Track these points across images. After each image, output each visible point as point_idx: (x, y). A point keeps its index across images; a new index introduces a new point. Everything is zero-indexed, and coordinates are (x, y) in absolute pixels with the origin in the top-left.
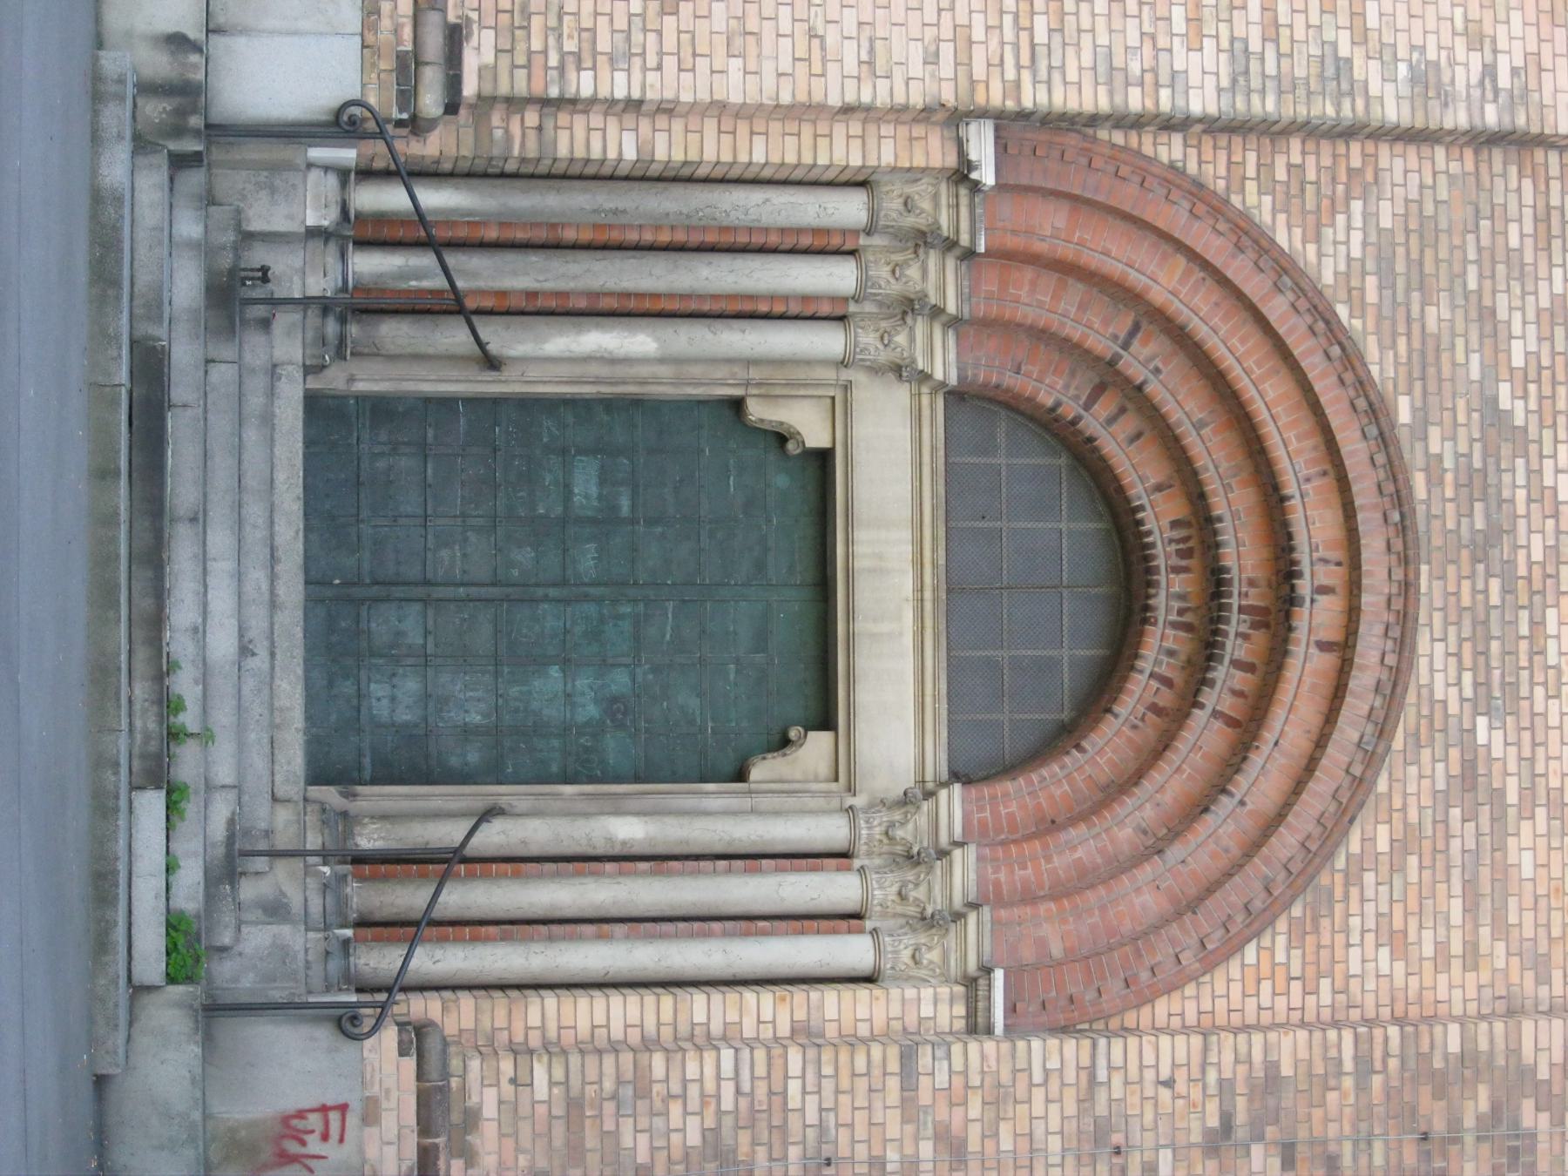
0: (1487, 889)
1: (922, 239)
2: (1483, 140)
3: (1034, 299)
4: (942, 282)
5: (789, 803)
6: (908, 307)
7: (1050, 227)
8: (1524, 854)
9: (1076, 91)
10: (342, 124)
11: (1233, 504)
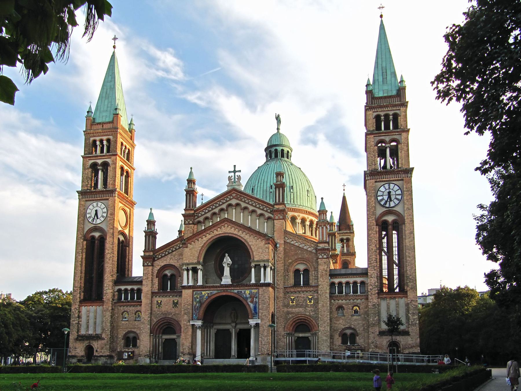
0: (178, 314)
1: (155, 336)
2: (151, 314)
3: (158, 332)
4: (157, 335)
5: (177, 340)
6: (158, 337)
7: (155, 332)
8: (177, 313)
9: (149, 331)
10: (150, 359)
11: (165, 324)
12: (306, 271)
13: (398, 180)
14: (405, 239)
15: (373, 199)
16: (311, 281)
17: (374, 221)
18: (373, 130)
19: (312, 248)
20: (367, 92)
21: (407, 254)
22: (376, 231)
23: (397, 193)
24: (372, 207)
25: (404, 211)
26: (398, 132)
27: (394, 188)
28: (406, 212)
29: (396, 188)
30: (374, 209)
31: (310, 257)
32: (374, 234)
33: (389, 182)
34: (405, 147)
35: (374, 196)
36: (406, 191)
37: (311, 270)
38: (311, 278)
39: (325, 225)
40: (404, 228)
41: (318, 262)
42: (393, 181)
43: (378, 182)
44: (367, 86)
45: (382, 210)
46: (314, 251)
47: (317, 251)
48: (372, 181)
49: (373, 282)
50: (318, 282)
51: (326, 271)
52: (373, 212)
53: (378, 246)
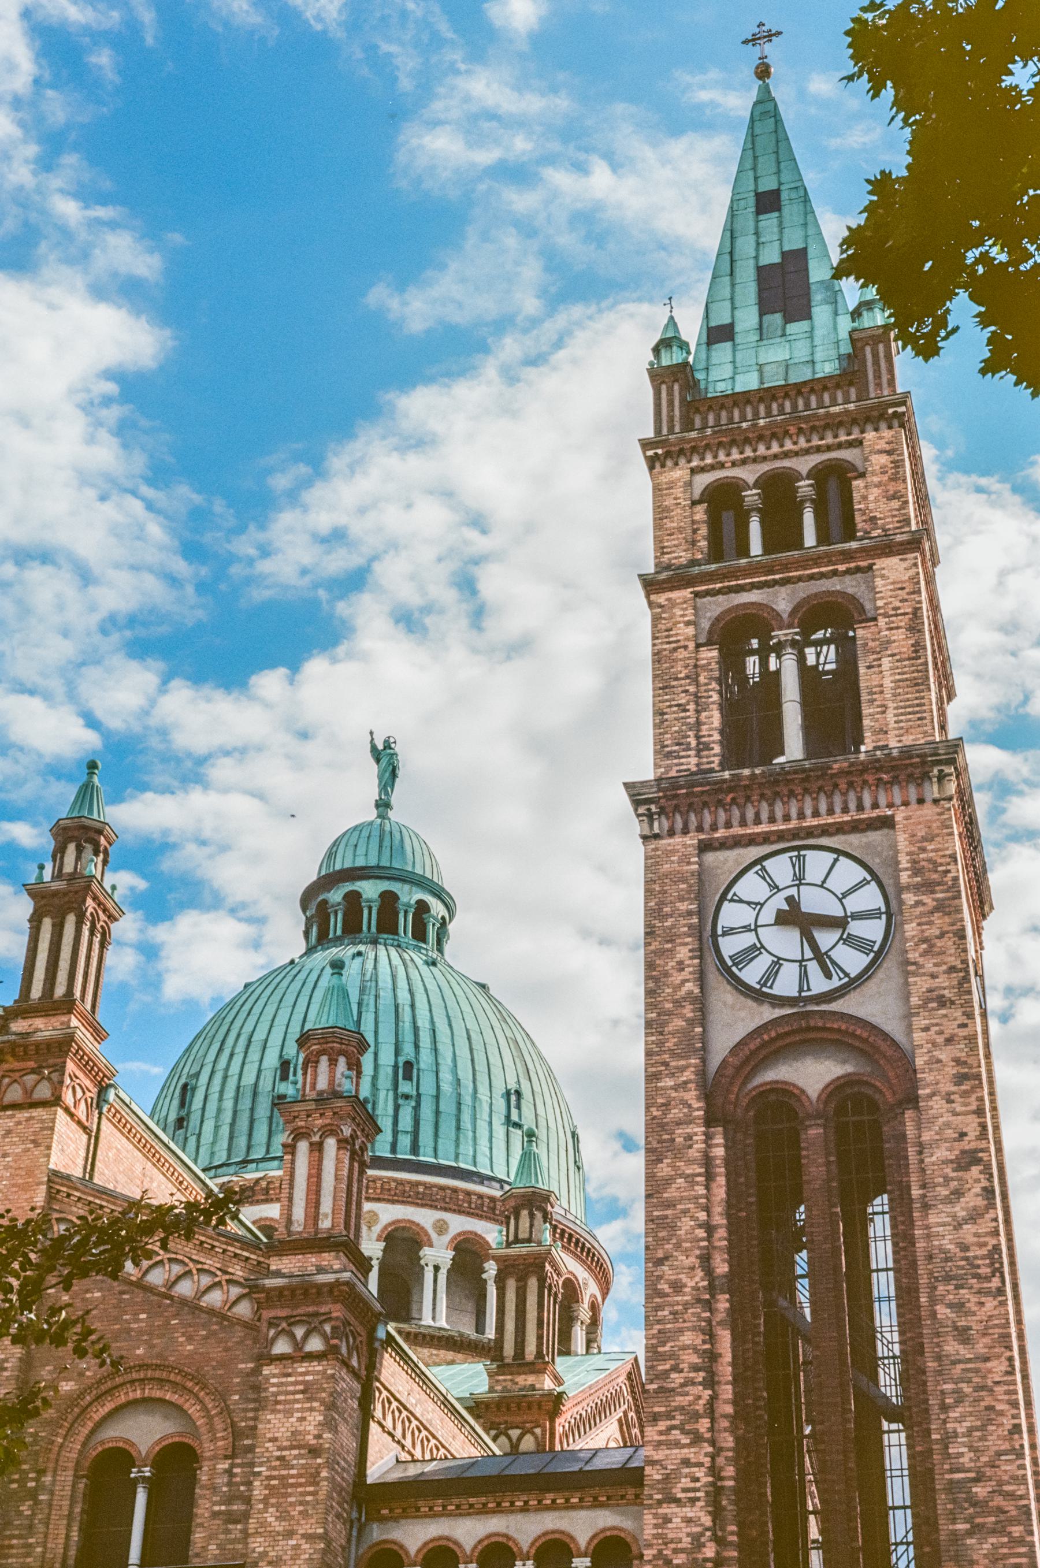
12: (177, 1462)
13: (856, 827)
14: (926, 1207)
15: (683, 953)
16: (198, 1536)
17: (691, 1096)
18: (693, 563)
19: (235, 1291)
20: (659, 376)
21: (942, 1311)
22: (707, 1161)
23: (856, 903)
24: (678, 1003)
25: (909, 1015)
26: (848, 556)
27: (833, 881)
28: (920, 1022)
29: (849, 873)
30: (688, 1011)
31: (216, 1352)
32: (690, 1179)
33: (797, 841)
34: (899, 635)
35: (698, 932)
36: (917, 888)
37: (207, 1449)
38: (205, 1507)
39: (330, 1131)
40: (910, 1131)
41: (257, 1388)
42: (825, 831)
43: (724, 845)
44: (656, 350)
45: (751, 1017)
46: (244, 1309)
47: (260, 1306)
48: (678, 840)
49: (679, 1531)
50: (245, 1534)
51: (314, 1452)
52: (685, 1034)
53: (722, 1268)
